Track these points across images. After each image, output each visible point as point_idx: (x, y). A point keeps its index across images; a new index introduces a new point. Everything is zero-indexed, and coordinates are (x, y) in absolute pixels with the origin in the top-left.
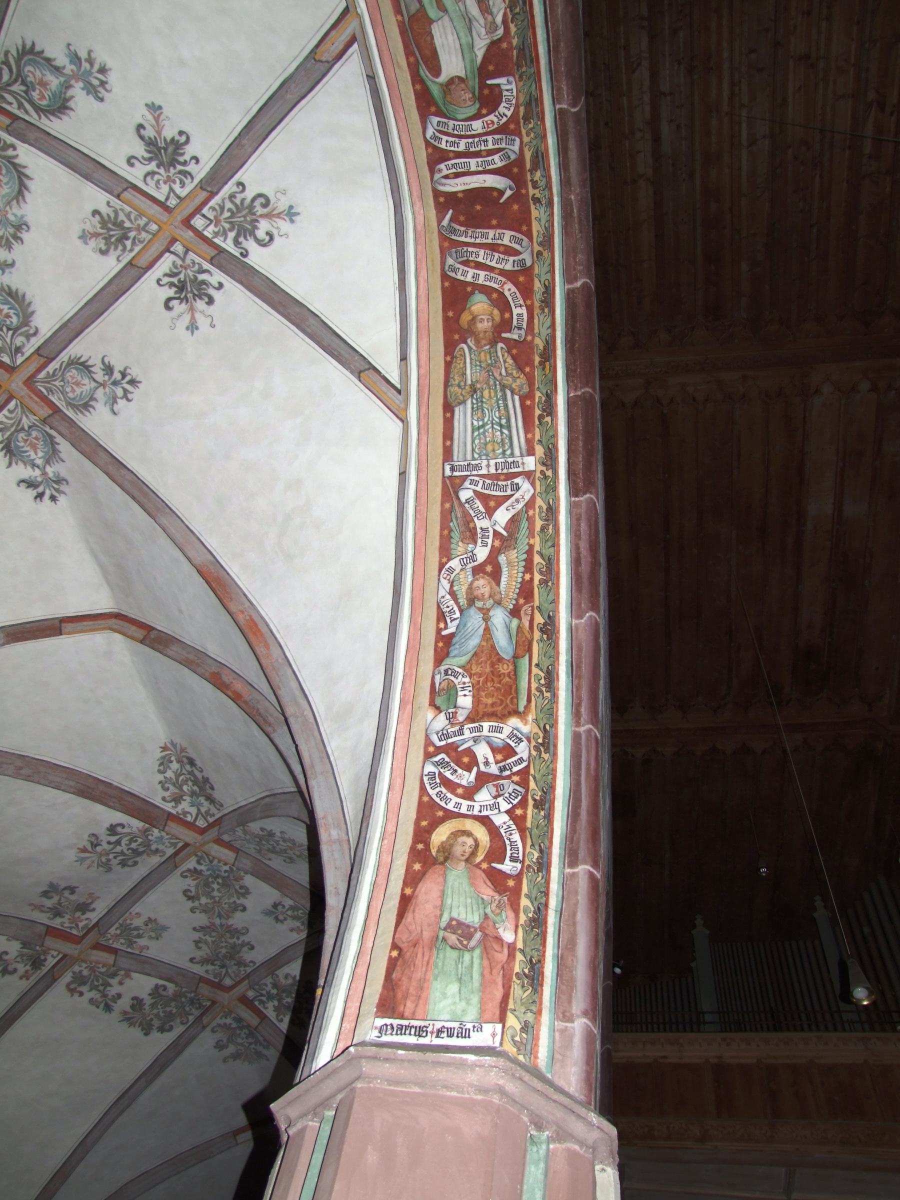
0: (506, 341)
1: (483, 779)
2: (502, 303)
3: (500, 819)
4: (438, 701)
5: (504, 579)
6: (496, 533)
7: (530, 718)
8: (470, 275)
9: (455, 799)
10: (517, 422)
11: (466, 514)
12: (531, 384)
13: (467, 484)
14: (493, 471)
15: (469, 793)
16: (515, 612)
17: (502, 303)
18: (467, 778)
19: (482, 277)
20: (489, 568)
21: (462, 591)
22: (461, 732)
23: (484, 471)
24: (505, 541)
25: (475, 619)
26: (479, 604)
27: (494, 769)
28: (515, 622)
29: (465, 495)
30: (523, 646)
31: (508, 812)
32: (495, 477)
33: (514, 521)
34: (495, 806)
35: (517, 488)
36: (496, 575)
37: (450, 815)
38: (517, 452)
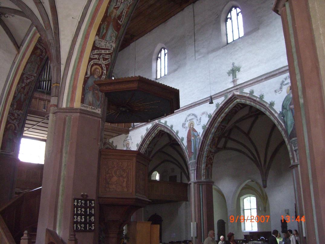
0: (40, 57)
1: (15, 118)
2: (42, 52)
3: (16, 125)
4: (12, 106)
5: (25, 90)
6: (27, 83)
7: (23, 111)
8: (39, 46)
9: (11, 121)
10: (36, 68)
11: (23, 79)
12: (40, 64)
13: (25, 75)
14: (30, 74)
15: (13, 120)
16: (25, 95)
17: (42, 52)
18: (13, 118)
19: (41, 48)
20: (24, 88)
21: (19, 90)
22: (14, 111)
23: (28, 74)
24: (27, 85)
25: (19, 95)
26: (21, 93)
27: (17, 117)
28: (25, 97)
29: (24, 76)
30: (25, 100)
31: (17, 124)
32: (29, 75)
33: (29, 83)
34: (16, 123)
35: (32, 77)
36: (24, 89)
37: (10, 123)
38: (34, 72)
